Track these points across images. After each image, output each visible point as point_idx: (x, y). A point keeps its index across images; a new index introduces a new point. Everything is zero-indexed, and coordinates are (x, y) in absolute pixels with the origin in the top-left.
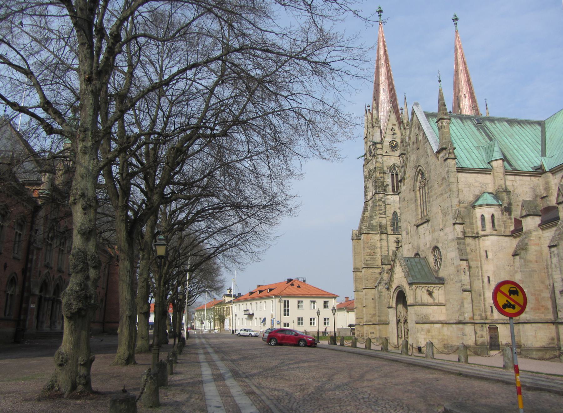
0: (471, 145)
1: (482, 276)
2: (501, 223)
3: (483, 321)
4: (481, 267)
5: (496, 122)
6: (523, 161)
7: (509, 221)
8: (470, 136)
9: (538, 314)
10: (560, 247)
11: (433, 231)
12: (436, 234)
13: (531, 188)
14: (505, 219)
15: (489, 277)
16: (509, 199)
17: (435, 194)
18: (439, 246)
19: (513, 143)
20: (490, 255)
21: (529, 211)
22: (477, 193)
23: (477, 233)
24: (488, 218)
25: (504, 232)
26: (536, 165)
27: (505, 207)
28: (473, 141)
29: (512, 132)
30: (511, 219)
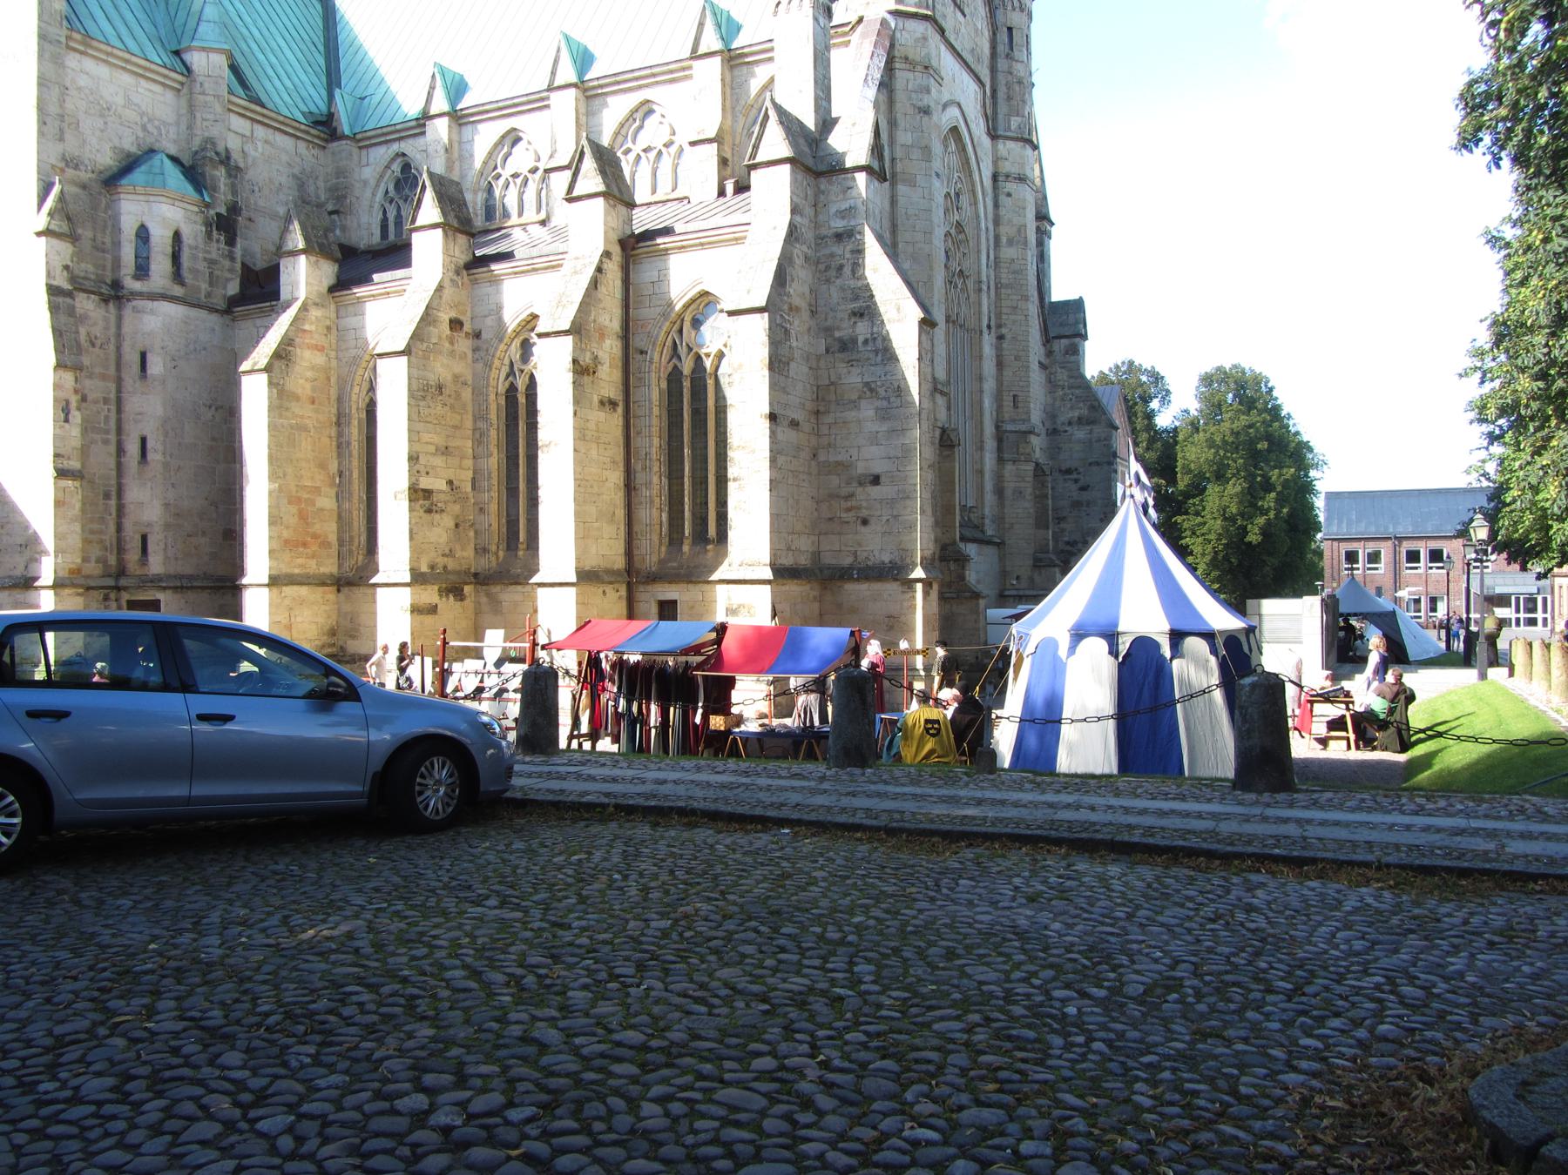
2: (202, 266)
3: (111, 582)
4: (119, 401)
7: (227, 263)
9: (300, 561)
10: (413, 359)
13: (294, 176)
14: (214, 256)
15: (144, 440)
16: (234, 192)
20: (156, 366)
21: (307, 239)
22: (129, 145)
23: (116, 285)
24: (160, 237)
25: (209, 295)
26: (314, 109)
27: (218, 215)
30: (232, 259)
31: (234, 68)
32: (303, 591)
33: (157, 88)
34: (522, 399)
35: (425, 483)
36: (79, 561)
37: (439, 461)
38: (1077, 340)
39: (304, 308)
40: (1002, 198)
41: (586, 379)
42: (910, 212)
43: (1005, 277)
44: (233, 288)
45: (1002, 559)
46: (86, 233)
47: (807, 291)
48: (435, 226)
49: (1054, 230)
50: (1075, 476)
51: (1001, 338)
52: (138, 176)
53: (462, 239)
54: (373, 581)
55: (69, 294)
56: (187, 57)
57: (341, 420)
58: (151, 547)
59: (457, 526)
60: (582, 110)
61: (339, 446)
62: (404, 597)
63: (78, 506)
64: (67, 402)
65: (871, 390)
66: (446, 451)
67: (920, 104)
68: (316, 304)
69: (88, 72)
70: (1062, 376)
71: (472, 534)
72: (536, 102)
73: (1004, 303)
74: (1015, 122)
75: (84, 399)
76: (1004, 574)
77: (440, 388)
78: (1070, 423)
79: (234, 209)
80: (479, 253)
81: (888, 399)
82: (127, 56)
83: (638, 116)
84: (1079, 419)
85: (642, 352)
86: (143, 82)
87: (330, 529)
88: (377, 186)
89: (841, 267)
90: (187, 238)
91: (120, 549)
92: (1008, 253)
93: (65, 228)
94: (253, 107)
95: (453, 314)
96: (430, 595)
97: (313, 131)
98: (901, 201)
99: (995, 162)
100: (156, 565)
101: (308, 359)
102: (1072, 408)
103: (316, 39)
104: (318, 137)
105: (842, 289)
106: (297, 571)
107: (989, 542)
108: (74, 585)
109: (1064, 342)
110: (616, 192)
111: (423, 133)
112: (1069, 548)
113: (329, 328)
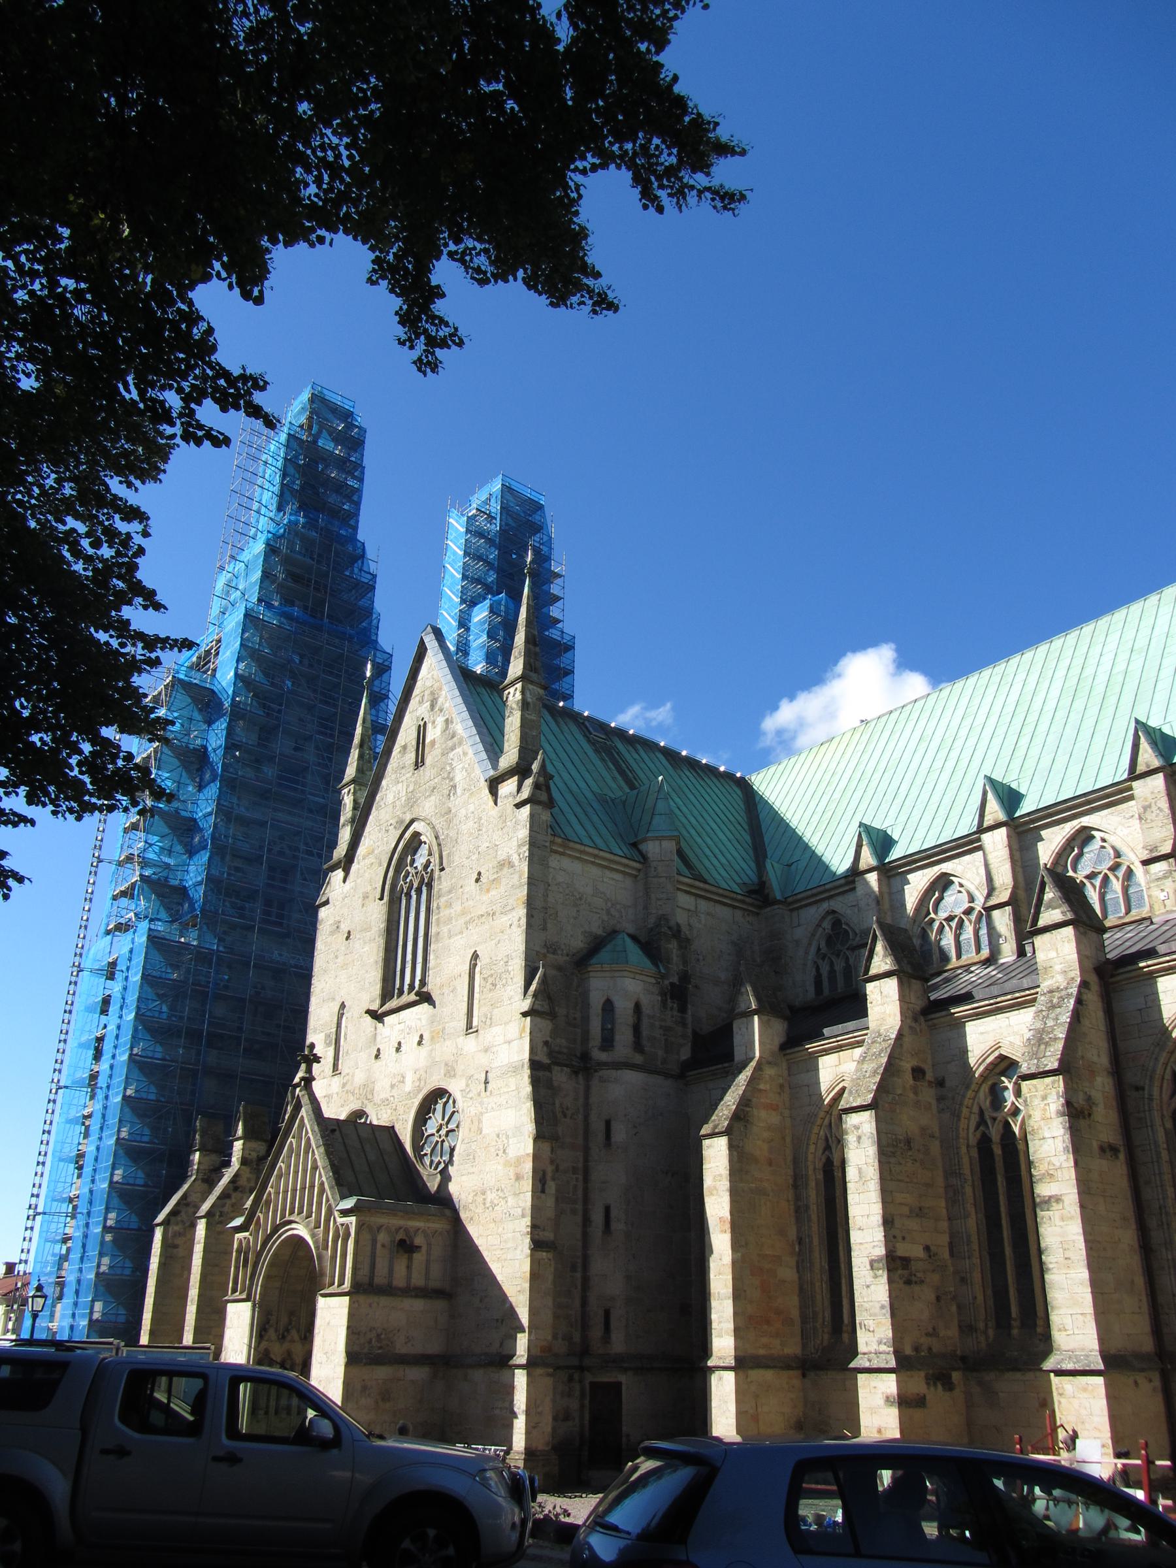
0: (582, 785)
1: (586, 1200)
5: (639, 747)
6: (715, 862)
8: (578, 763)
9: (764, 1340)
11: (439, 1035)
12: (445, 1049)
15: (607, 1209)
16: (685, 962)
17: (463, 913)
18: (454, 1087)
19: (684, 809)
20: (620, 1134)
22: (596, 928)
23: (585, 1057)
24: (624, 1008)
26: (746, 880)
27: (672, 984)
28: (587, 776)
29: (679, 782)
31: (680, 853)
32: (768, 1375)
33: (619, 877)
34: (997, 1151)
35: (902, 1250)
36: (550, 1338)
37: (913, 1224)
39: (759, 1063)
41: (1083, 1123)
44: (685, 1053)
46: (561, 1011)
48: (887, 975)
52: (604, 955)
53: (916, 985)
54: (852, 1365)
55: (547, 1068)
56: (642, 847)
57: (798, 1182)
58: (614, 1324)
59: (938, 1299)
60: (1015, 846)
61: (797, 1210)
62: (889, 1384)
63: (551, 1278)
64: (544, 1173)
66: (919, 1212)
68: (769, 1063)
69: (564, 867)
71: (954, 1308)
72: (968, 844)
75: (557, 1169)
77: (908, 1142)
79: (685, 977)
80: (934, 996)
82: (596, 852)
83: (1078, 841)
85: (1137, 1089)
86: (607, 872)
87: (791, 1303)
88: (810, 944)
90: (646, 1010)
91: (585, 1326)
93: (546, 1008)
94: (698, 884)
95: (915, 1062)
96: (918, 1385)
97: (748, 900)
100: (618, 1344)
101: (764, 1118)
103: (739, 818)
104: (752, 905)
106: (762, 1352)
108: (545, 1365)
110: (1085, 918)
111: (854, 889)
113: (781, 1086)
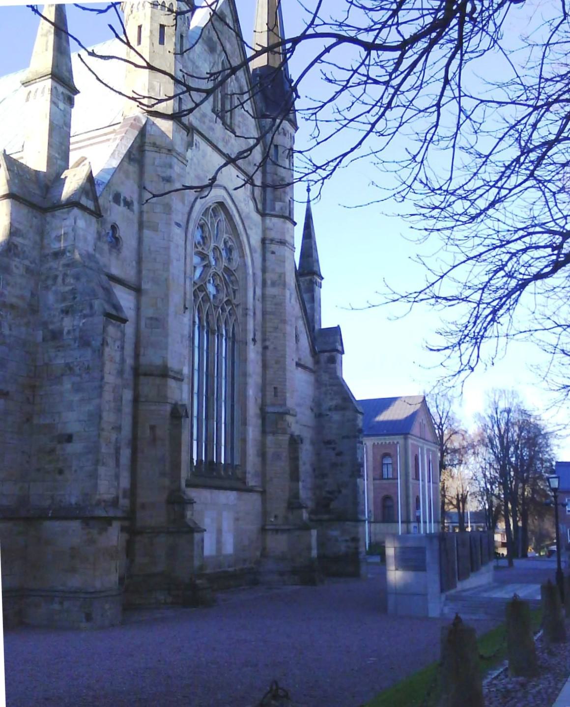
38: (335, 353)
40: (269, 256)
42: (152, 249)
43: (269, 307)
45: (264, 502)
47: (27, 294)
49: (323, 282)
50: (333, 446)
51: (265, 348)
65: (71, 369)
67: (164, 175)
70: (325, 377)
73: (269, 324)
74: (278, 205)
76: (265, 514)
78: (330, 410)
81: (80, 375)
84: (336, 406)
89: (56, 277)
92: (271, 291)
98: (146, 240)
99: (265, 230)
102: (332, 399)
105: (56, 292)
107: (250, 490)
109: (327, 354)
112: (329, 496)
